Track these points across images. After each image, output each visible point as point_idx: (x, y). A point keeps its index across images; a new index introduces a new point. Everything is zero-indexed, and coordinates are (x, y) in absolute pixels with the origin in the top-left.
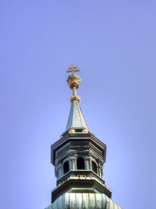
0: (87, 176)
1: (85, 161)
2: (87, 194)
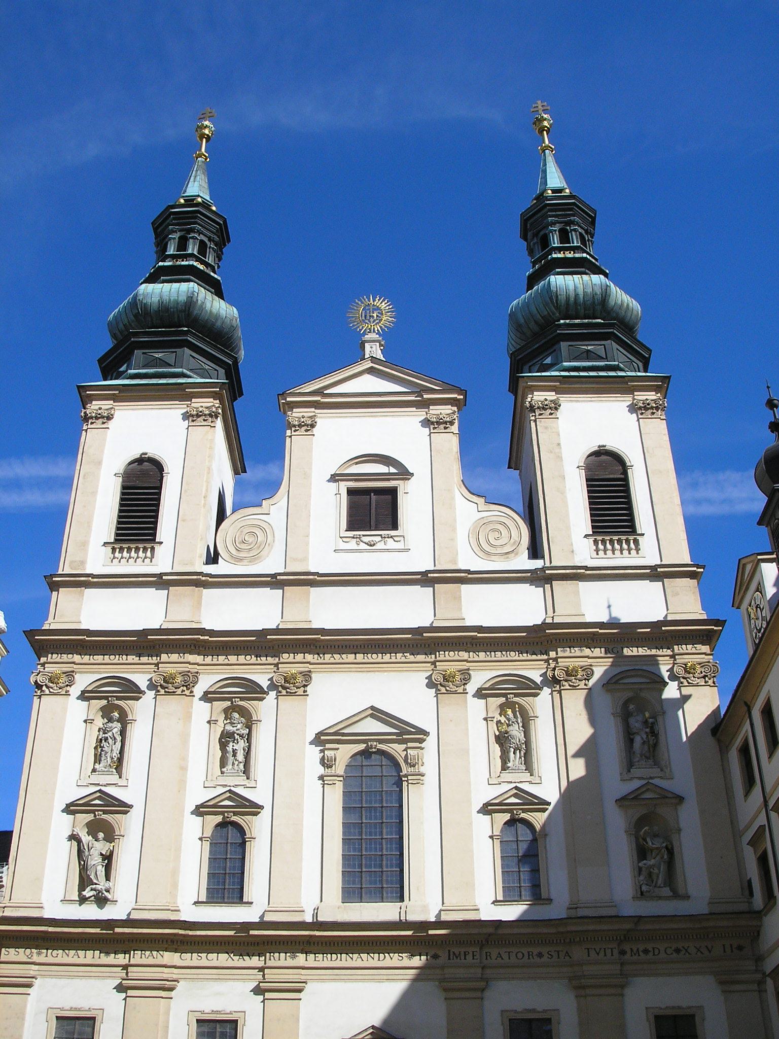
0: (574, 253)
2: (579, 276)
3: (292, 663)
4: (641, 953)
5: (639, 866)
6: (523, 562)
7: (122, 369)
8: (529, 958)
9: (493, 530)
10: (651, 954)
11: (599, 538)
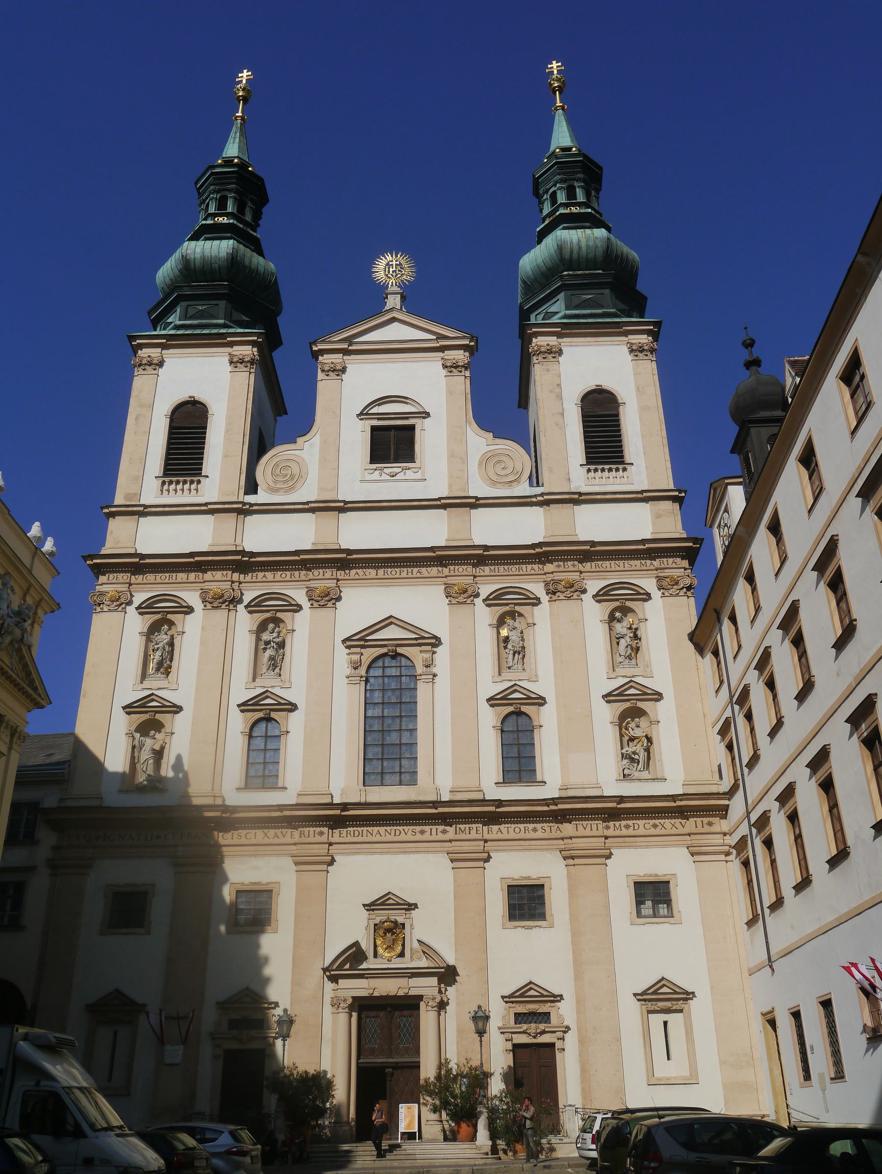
1: (578, 190)
2: (582, 230)
3: (323, 579)
4: (623, 828)
5: (622, 753)
6: (523, 489)
7: (169, 321)
8: (525, 833)
9: (499, 462)
10: (632, 828)
11: (592, 467)
